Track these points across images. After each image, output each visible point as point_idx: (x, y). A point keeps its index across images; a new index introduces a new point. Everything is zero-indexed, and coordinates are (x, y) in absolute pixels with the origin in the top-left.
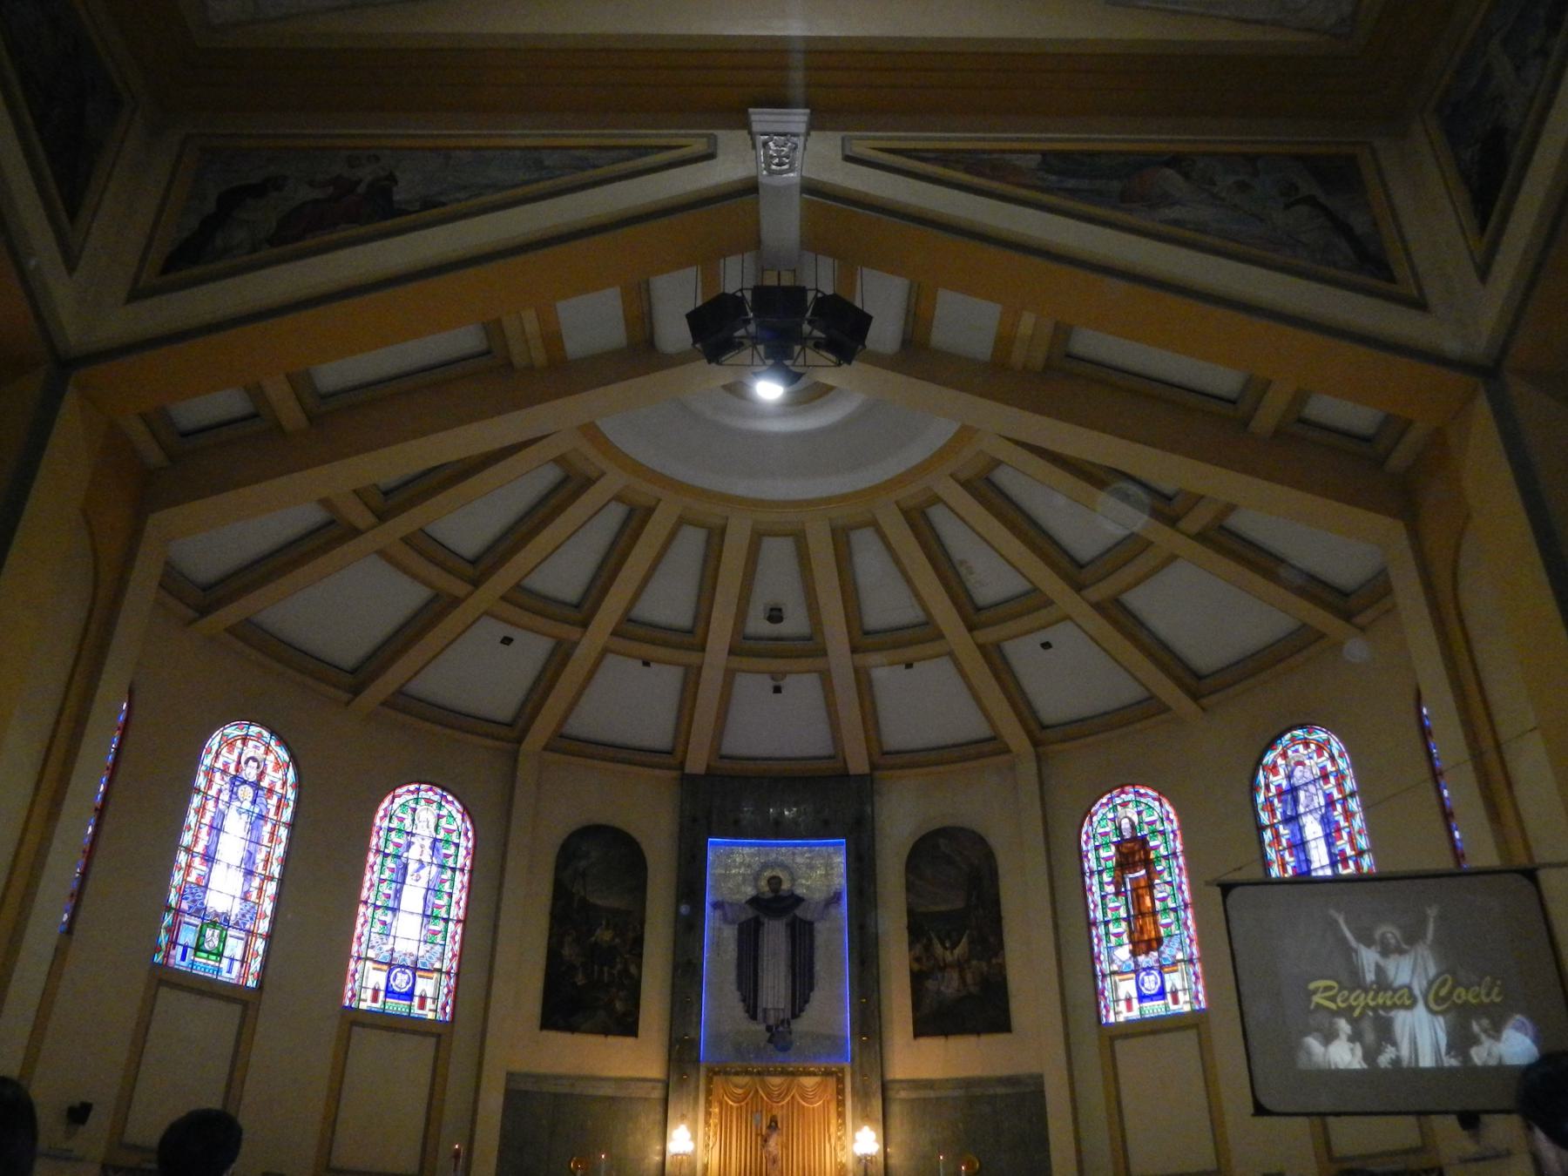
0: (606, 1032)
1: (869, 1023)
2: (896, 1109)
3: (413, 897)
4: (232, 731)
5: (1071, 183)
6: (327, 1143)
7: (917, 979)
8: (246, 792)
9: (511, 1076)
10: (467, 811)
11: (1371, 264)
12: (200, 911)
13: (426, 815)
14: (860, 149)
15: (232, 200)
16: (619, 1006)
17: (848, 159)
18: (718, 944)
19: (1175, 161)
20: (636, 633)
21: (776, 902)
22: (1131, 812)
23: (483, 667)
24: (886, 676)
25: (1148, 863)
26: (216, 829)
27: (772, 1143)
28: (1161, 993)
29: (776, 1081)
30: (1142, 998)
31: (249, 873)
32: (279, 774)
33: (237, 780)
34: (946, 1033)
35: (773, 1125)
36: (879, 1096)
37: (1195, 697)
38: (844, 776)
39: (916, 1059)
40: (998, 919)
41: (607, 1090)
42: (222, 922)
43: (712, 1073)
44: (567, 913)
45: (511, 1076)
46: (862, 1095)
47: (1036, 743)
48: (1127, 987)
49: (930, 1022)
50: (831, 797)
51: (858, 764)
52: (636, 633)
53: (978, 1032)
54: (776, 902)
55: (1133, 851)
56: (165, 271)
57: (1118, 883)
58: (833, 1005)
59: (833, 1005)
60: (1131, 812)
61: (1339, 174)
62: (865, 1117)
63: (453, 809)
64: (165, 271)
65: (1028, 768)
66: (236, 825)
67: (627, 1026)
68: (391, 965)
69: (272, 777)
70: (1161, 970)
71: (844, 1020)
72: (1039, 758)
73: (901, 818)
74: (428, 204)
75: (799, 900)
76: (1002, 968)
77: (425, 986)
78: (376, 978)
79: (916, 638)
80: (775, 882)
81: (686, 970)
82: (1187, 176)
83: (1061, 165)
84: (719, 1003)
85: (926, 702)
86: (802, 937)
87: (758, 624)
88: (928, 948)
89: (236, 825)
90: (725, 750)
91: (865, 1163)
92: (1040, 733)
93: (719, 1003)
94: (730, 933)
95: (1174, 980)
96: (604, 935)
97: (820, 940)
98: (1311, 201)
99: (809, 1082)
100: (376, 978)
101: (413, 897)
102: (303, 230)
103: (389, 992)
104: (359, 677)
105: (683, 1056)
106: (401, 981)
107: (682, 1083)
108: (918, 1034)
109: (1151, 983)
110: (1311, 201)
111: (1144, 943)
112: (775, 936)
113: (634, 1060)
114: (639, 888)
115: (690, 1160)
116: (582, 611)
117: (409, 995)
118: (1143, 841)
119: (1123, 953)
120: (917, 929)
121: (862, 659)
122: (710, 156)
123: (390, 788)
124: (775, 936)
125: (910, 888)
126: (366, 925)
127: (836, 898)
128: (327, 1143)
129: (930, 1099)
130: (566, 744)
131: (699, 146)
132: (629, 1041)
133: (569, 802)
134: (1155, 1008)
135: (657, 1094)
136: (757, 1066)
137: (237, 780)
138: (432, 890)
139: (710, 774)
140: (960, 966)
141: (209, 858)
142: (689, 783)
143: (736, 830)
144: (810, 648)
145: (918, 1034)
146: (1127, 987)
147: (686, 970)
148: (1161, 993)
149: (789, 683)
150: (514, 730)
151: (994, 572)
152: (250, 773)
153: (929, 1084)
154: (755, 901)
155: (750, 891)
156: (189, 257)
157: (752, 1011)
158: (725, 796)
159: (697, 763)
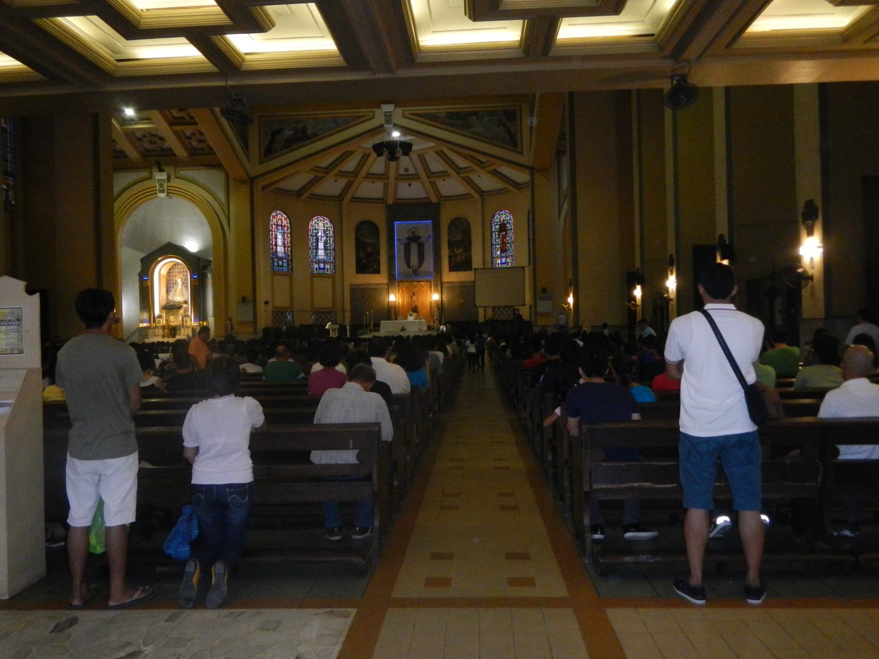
0: (372, 273)
1: (438, 270)
2: (444, 289)
3: (321, 245)
4: (274, 214)
5: (452, 122)
6: (312, 303)
7: (450, 257)
8: (280, 228)
9: (351, 285)
10: (331, 222)
11: (513, 142)
12: (277, 257)
13: (321, 224)
14: (406, 113)
15: (275, 134)
16: (375, 267)
17: (404, 117)
18: (399, 249)
19: (475, 114)
20: (370, 176)
21: (414, 238)
22: (504, 216)
23: (331, 186)
24: (440, 183)
25: (506, 231)
26: (276, 238)
27: (414, 298)
28: (505, 263)
29: (415, 283)
30: (502, 264)
31: (284, 247)
32: (285, 222)
33: (277, 225)
34: (457, 271)
35: (414, 294)
36: (440, 286)
37: (518, 189)
38: (431, 203)
39: (450, 277)
40: (470, 243)
41: (374, 287)
42: (281, 259)
43: (399, 282)
44: (360, 245)
45: (351, 285)
46: (436, 285)
47: (481, 196)
48: (499, 261)
49: (454, 268)
50: (426, 209)
51: (434, 200)
52: (370, 176)
53: (464, 270)
54: (414, 238)
55: (503, 227)
56: (266, 155)
57: (499, 235)
58: (429, 264)
59: (429, 264)
60: (504, 216)
61: (511, 115)
62: (437, 291)
63: (327, 221)
64: (266, 155)
65: (479, 202)
66: (280, 237)
67: (378, 271)
68: (319, 262)
69: (285, 222)
70: (507, 257)
71: (431, 269)
72: (483, 200)
73: (447, 215)
74: (316, 135)
75: (419, 238)
76: (470, 256)
77: (327, 266)
78: (316, 266)
79: (443, 174)
80: (413, 233)
81: (391, 258)
82: (477, 118)
83: (451, 116)
84: (399, 265)
85: (451, 186)
86: (421, 247)
87: (402, 172)
88: (453, 250)
89: (280, 237)
90: (398, 197)
91: (436, 302)
92: (482, 193)
93: (399, 265)
94: (402, 247)
95: (509, 260)
96: (369, 250)
97: (426, 247)
98: (504, 125)
99: (423, 283)
100: (316, 266)
101: (321, 245)
102: (290, 144)
103: (320, 268)
104: (300, 193)
105: (392, 278)
106: (322, 265)
107: (392, 284)
108: (450, 271)
109: (504, 260)
110: (504, 125)
111: (503, 250)
112: (414, 248)
113: (380, 279)
114: (377, 236)
115: (395, 302)
116: (356, 173)
117: (324, 269)
118: (505, 225)
119: (499, 253)
120: (451, 245)
121: (432, 180)
122: (373, 118)
123: (311, 218)
124: (414, 248)
125: (449, 234)
126: (311, 254)
127: (429, 237)
128: (312, 303)
129: (452, 286)
130: (356, 200)
131: (371, 115)
132: (378, 275)
133: (355, 215)
134: (504, 266)
135: (386, 287)
136: (410, 279)
137: (277, 225)
138: (325, 243)
139: (394, 204)
140: (461, 254)
141: (276, 245)
142: (388, 206)
143: (402, 219)
144: (416, 177)
145: (450, 271)
146: (499, 261)
147: (391, 258)
148: (505, 263)
149: (413, 184)
150: (340, 198)
151: (461, 163)
152: (280, 223)
153: (453, 283)
154: (408, 238)
155: (407, 236)
156: (269, 152)
157: (409, 267)
158: (400, 210)
159: (390, 201)
